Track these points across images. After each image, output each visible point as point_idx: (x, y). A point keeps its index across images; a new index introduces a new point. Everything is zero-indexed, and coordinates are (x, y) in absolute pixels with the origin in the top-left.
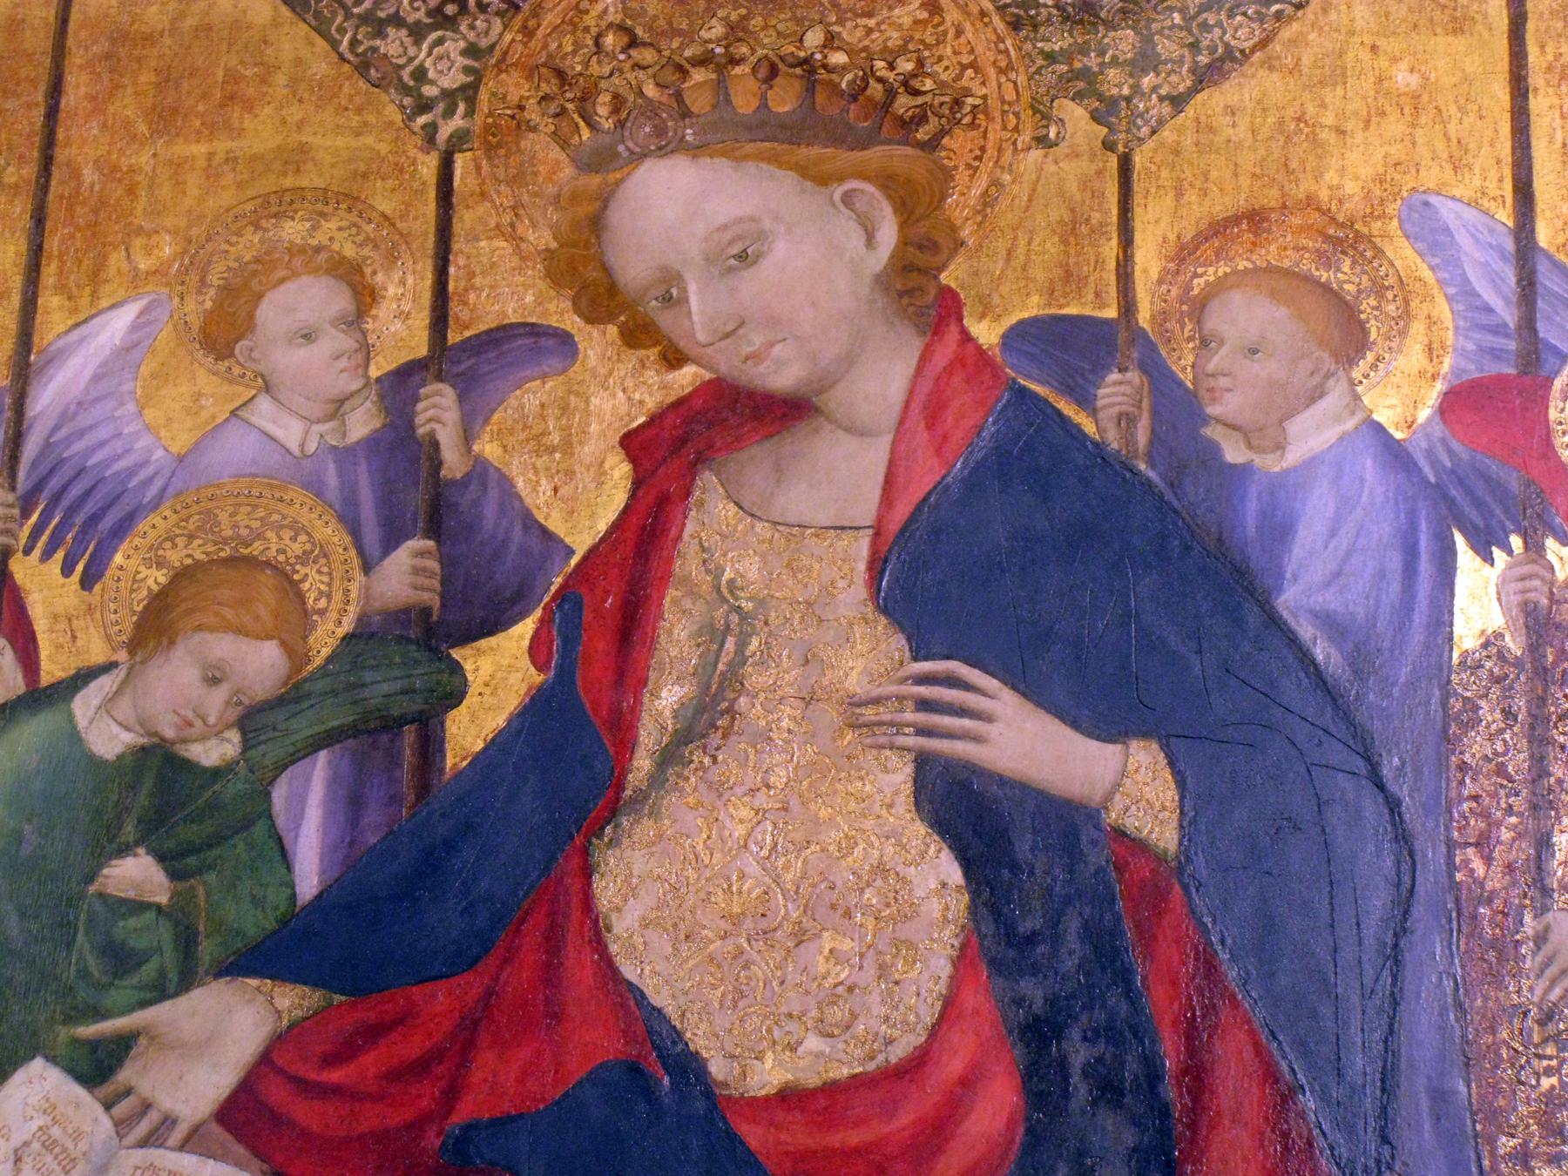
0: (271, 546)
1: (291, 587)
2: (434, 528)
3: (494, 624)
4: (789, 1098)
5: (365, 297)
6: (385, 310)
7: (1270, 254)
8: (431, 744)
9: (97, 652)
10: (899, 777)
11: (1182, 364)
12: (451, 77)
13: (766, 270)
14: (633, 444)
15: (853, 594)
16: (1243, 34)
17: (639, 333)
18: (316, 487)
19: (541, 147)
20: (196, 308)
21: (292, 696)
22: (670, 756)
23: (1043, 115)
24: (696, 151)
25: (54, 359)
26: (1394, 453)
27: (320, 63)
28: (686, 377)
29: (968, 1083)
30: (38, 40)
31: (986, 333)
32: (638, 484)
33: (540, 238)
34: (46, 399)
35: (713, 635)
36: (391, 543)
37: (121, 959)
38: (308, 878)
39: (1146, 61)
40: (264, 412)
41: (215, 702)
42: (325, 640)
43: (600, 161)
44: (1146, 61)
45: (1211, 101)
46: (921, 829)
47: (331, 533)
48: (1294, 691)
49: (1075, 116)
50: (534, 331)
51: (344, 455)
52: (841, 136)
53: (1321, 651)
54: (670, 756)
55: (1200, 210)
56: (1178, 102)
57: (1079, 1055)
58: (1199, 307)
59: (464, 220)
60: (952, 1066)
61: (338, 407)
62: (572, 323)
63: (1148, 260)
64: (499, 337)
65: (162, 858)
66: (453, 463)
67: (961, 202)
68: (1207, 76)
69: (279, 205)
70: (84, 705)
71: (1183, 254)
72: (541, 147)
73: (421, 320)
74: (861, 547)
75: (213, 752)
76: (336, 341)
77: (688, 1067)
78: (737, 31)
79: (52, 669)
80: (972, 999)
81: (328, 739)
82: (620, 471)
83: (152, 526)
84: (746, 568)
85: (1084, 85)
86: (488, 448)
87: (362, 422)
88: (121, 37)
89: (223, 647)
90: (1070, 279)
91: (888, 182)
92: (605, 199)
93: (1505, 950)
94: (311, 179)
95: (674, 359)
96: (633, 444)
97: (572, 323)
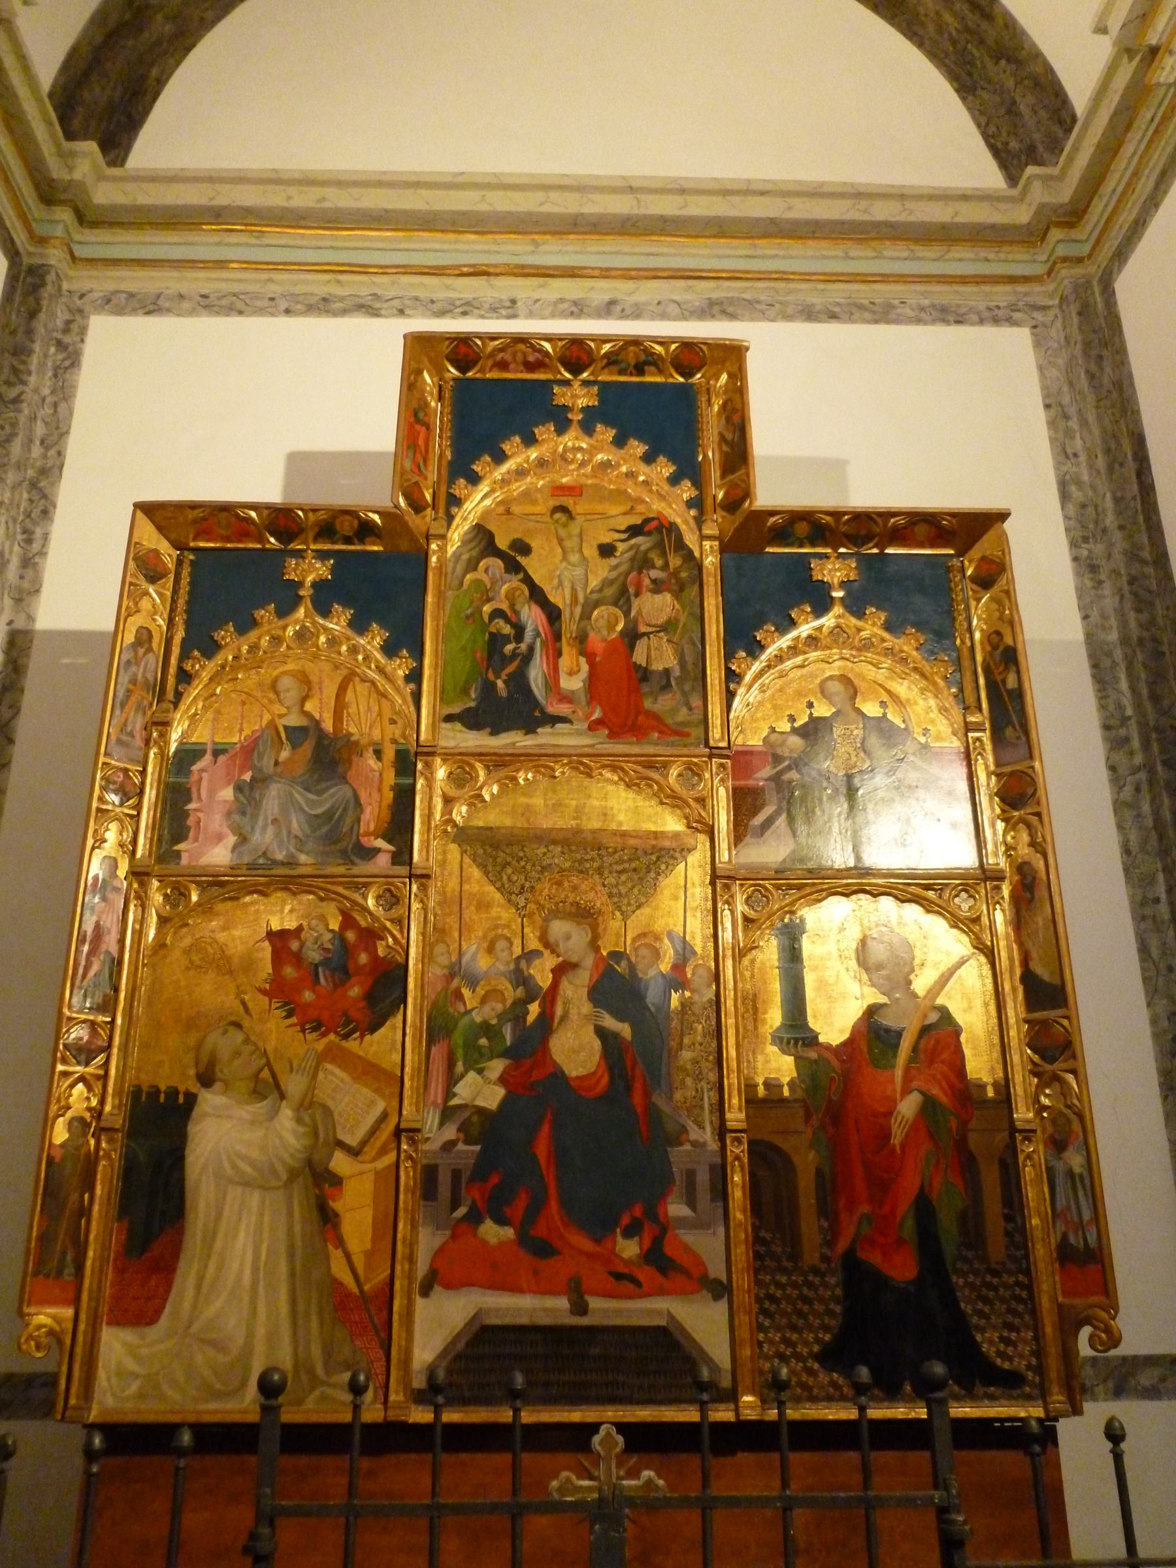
0: (500, 987)
1: (503, 994)
2: (524, 984)
3: (532, 1001)
4: (578, 1078)
5: (511, 944)
6: (514, 947)
7: (647, 941)
8: (525, 1020)
9: (475, 1005)
10: (591, 1028)
11: (633, 959)
12: (522, 904)
13: (572, 941)
14: (553, 971)
15: (585, 996)
16: (643, 900)
17: (553, 952)
18: (505, 977)
19: (537, 917)
20: (485, 945)
21: (505, 1012)
22: (560, 1023)
23: (613, 914)
24: (560, 919)
25: (465, 953)
26: (663, 976)
27: (502, 901)
28: (561, 959)
29: (602, 1077)
30: (457, 894)
31: (605, 954)
32: (554, 978)
33: (538, 934)
34: (465, 960)
35: (565, 1004)
36: (517, 987)
37: (481, 1055)
38: (508, 1043)
39: (629, 904)
40: (497, 964)
41: (493, 1013)
42: (509, 1003)
43: (546, 920)
44: (629, 904)
45: (638, 912)
46: (594, 1036)
47: (510, 987)
48: (648, 1014)
49: (618, 914)
50: (537, 951)
51: (510, 972)
52: (584, 917)
53: (653, 1009)
54: (560, 1023)
55: (637, 932)
56: (634, 912)
57: (616, 1071)
58: (636, 949)
59: (526, 930)
60: (600, 1073)
61: (508, 964)
62: (542, 949)
63: (629, 942)
64: (532, 952)
65: (489, 1039)
66: (526, 973)
67: (600, 930)
68: (638, 907)
69: (496, 927)
70: (474, 1013)
71: (634, 940)
72: (537, 917)
73: (520, 949)
74: (586, 990)
75: (494, 1022)
76: (506, 953)
77: (563, 1073)
78: (567, 896)
79: (469, 1007)
80: (603, 1063)
81: (509, 1020)
82: (551, 976)
83: (482, 983)
84: (569, 993)
85: (619, 909)
86: (532, 971)
87: (512, 966)
88: (470, 894)
89: (494, 1004)
90: (617, 944)
91: (589, 925)
92: (547, 927)
93: (676, 1056)
94: (503, 922)
95: (558, 956)
96: (553, 971)
97: (542, 949)
